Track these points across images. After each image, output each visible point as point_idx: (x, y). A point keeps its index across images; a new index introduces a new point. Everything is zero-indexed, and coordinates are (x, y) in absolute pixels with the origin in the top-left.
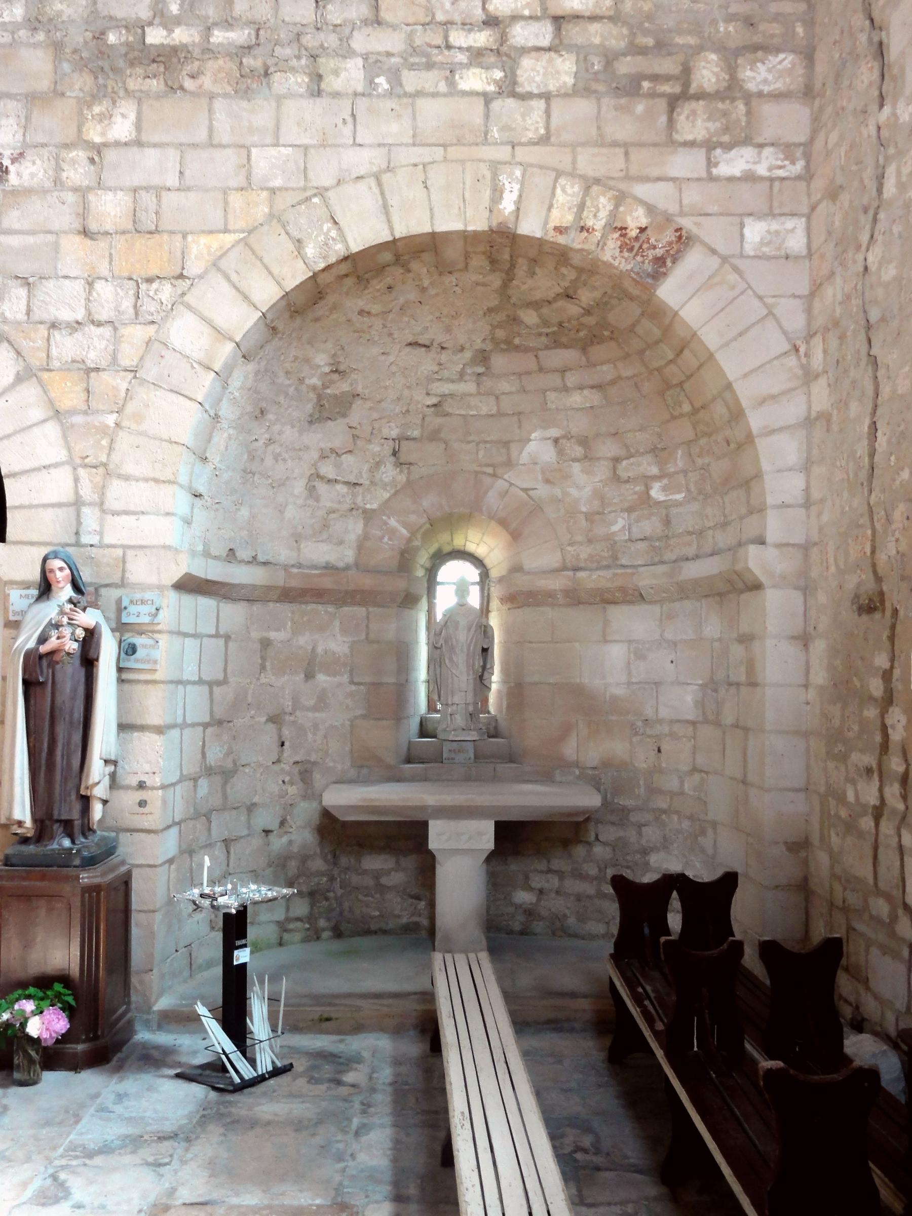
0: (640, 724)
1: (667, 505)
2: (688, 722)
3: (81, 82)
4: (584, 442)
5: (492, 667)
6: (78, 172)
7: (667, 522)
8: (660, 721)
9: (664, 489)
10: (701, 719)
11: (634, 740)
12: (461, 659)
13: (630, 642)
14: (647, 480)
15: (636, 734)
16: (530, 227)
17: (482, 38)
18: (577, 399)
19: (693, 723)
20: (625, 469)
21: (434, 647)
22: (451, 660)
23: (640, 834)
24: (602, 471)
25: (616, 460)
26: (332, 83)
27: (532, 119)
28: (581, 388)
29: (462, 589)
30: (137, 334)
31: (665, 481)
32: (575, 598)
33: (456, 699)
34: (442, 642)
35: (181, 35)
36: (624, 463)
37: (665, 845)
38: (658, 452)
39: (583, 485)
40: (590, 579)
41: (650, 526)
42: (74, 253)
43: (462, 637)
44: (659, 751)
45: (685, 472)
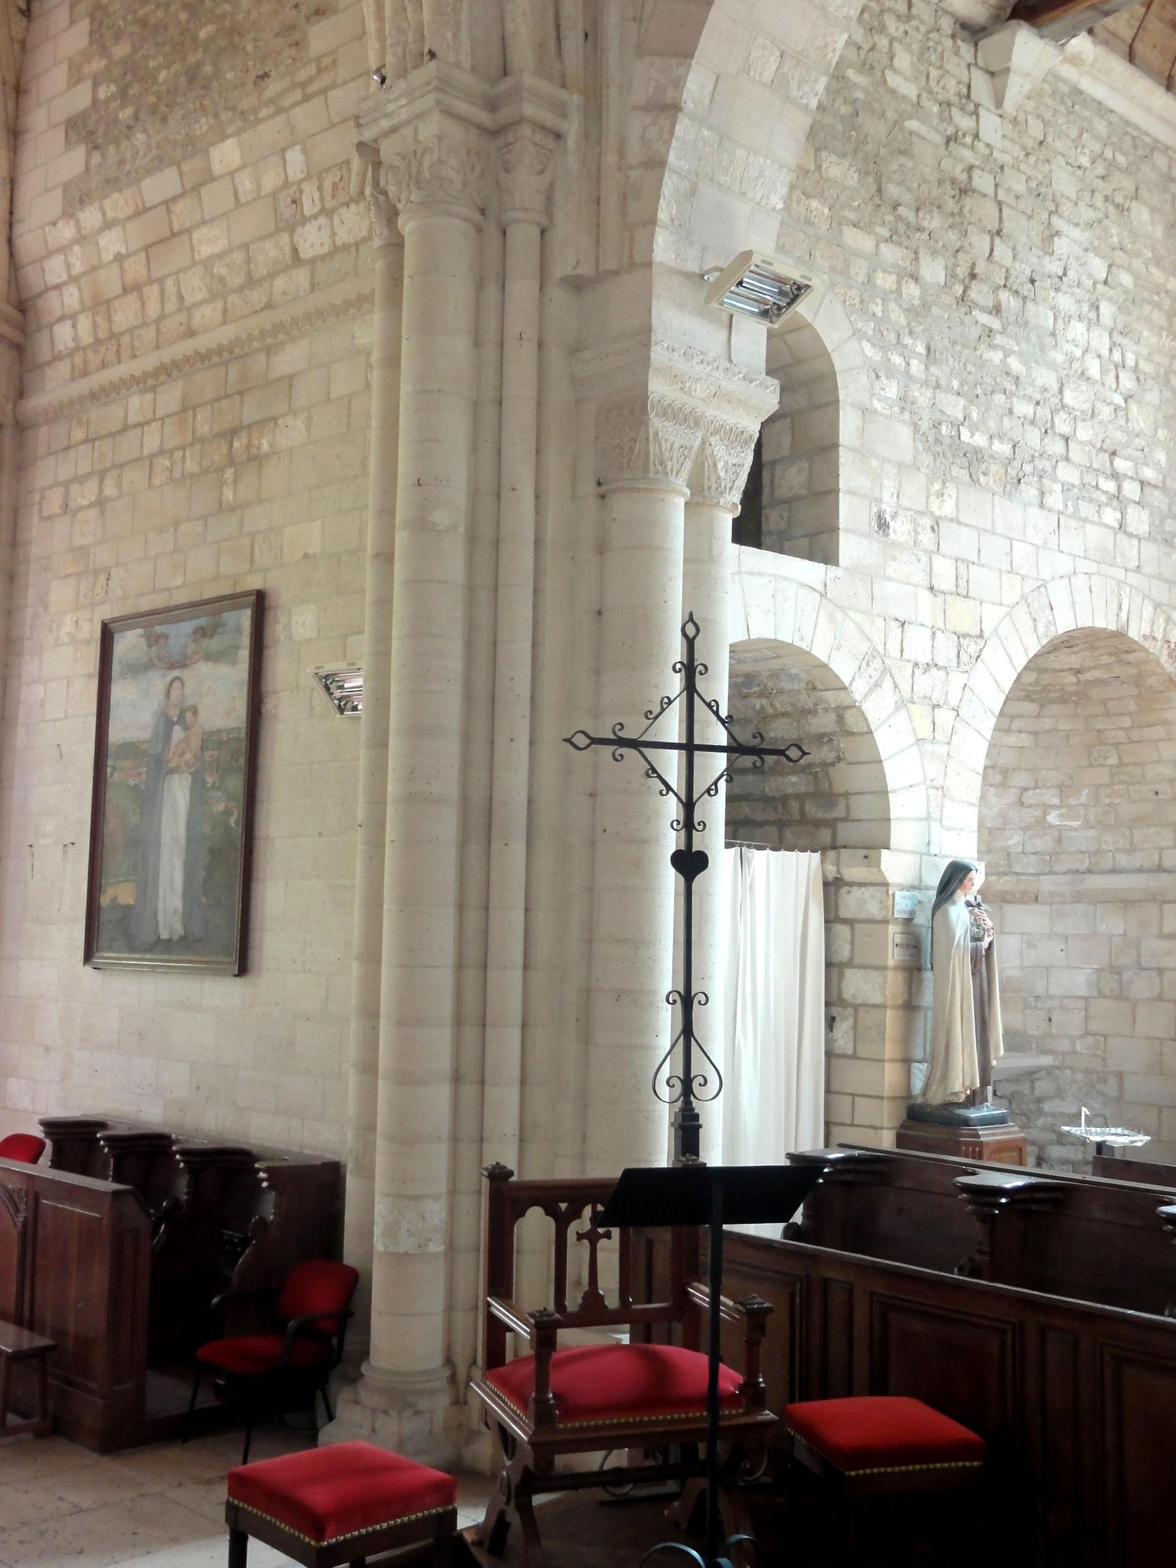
0: (1032, 999)
1: (1060, 829)
2: (1080, 997)
3: (926, 459)
4: (1005, 772)
6: (926, 538)
7: (1059, 841)
8: (1051, 997)
9: (1060, 816)
10: (1095, 994)
11: (1026, 1012)
13: (1023, 934)
14: (1046, 808)
15: (1029, 1007)
16: (1133, 634)
17: (1110, 486)
19: (1086, 999)
20: (1030, 797)
23: (1033, 1088)
24: (1011, 796)
25: (1026, 789)
26: (1050, 501)
27: (1130, 548)
28: (1020, 731)
30: (957, 679)
31: (1063, 811)
35: (980, 440)
36: (1030, 792)
38: (1061, 788)
41: (1043, 843)
42: (925, 608)
44: (1050, 1020)
45: (1085, 806)
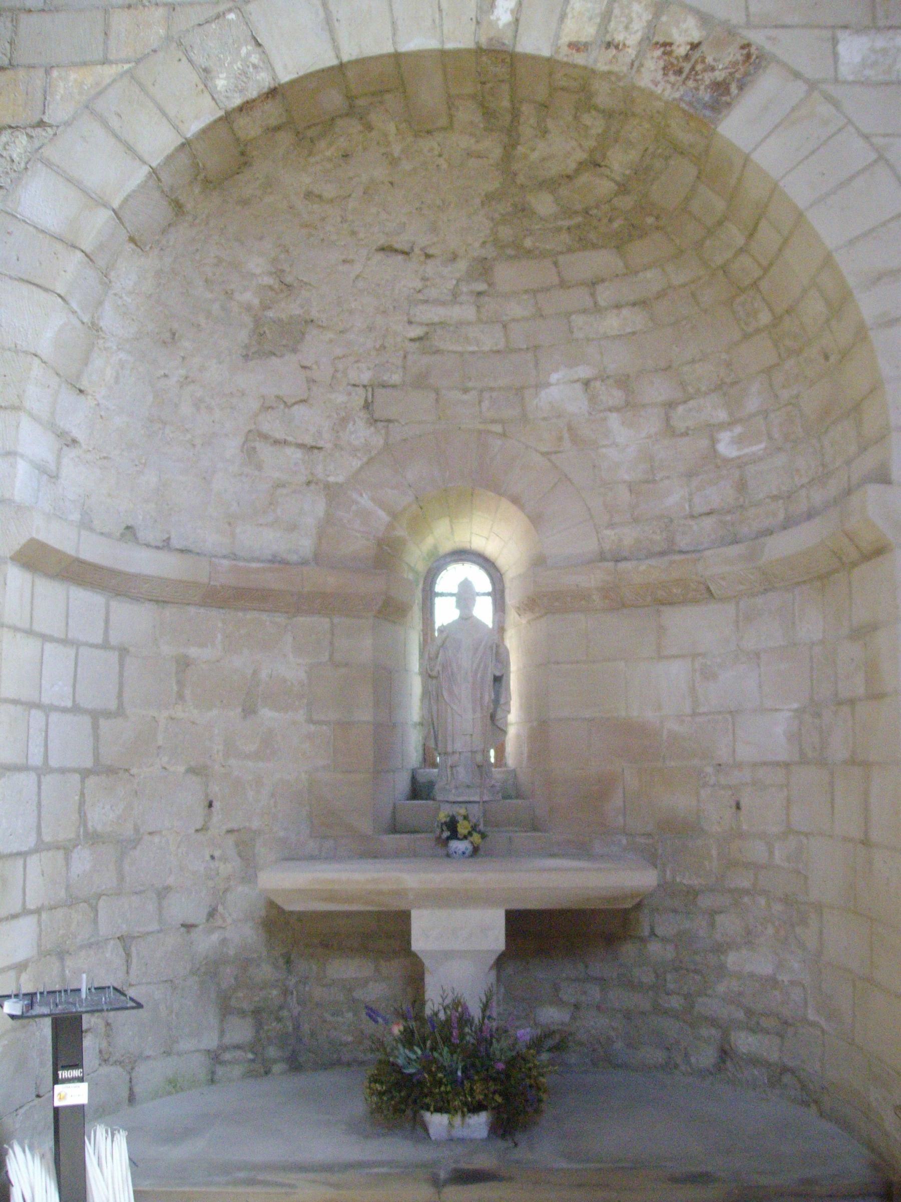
0: (709, 770)
1: (741, 464)
2: (777, 764)
4: (623, 382)
5: (507, 703)
7: (742, 486)
8: (739, 766)
9: (739, 441)
10: (797, 758)
11: (703, 792)
12: (464, 691)
13: (695, 656)
14: (711, 430)
15: (705, 785)
16: (534, 43)
18: (612, 323)
19: (787, 765)
20: (681, 417)
21: (428, 676)
22: (451, 693)
23: (712, 925)
24: (652, 423)
25: (671, 405)
28: (618, 307)
29: (465, 596)
31: (738, 429)
32: (616, 600)
33: (458, 746)
34: (438, 668)
36: (680, 409)
37: (749, 939)
38: (727, 388)
39: (625, 442)
40: (639, 572)
41: (719, 494)
43: (466, 662)
44: (738, 807)
45: (765, 413)
